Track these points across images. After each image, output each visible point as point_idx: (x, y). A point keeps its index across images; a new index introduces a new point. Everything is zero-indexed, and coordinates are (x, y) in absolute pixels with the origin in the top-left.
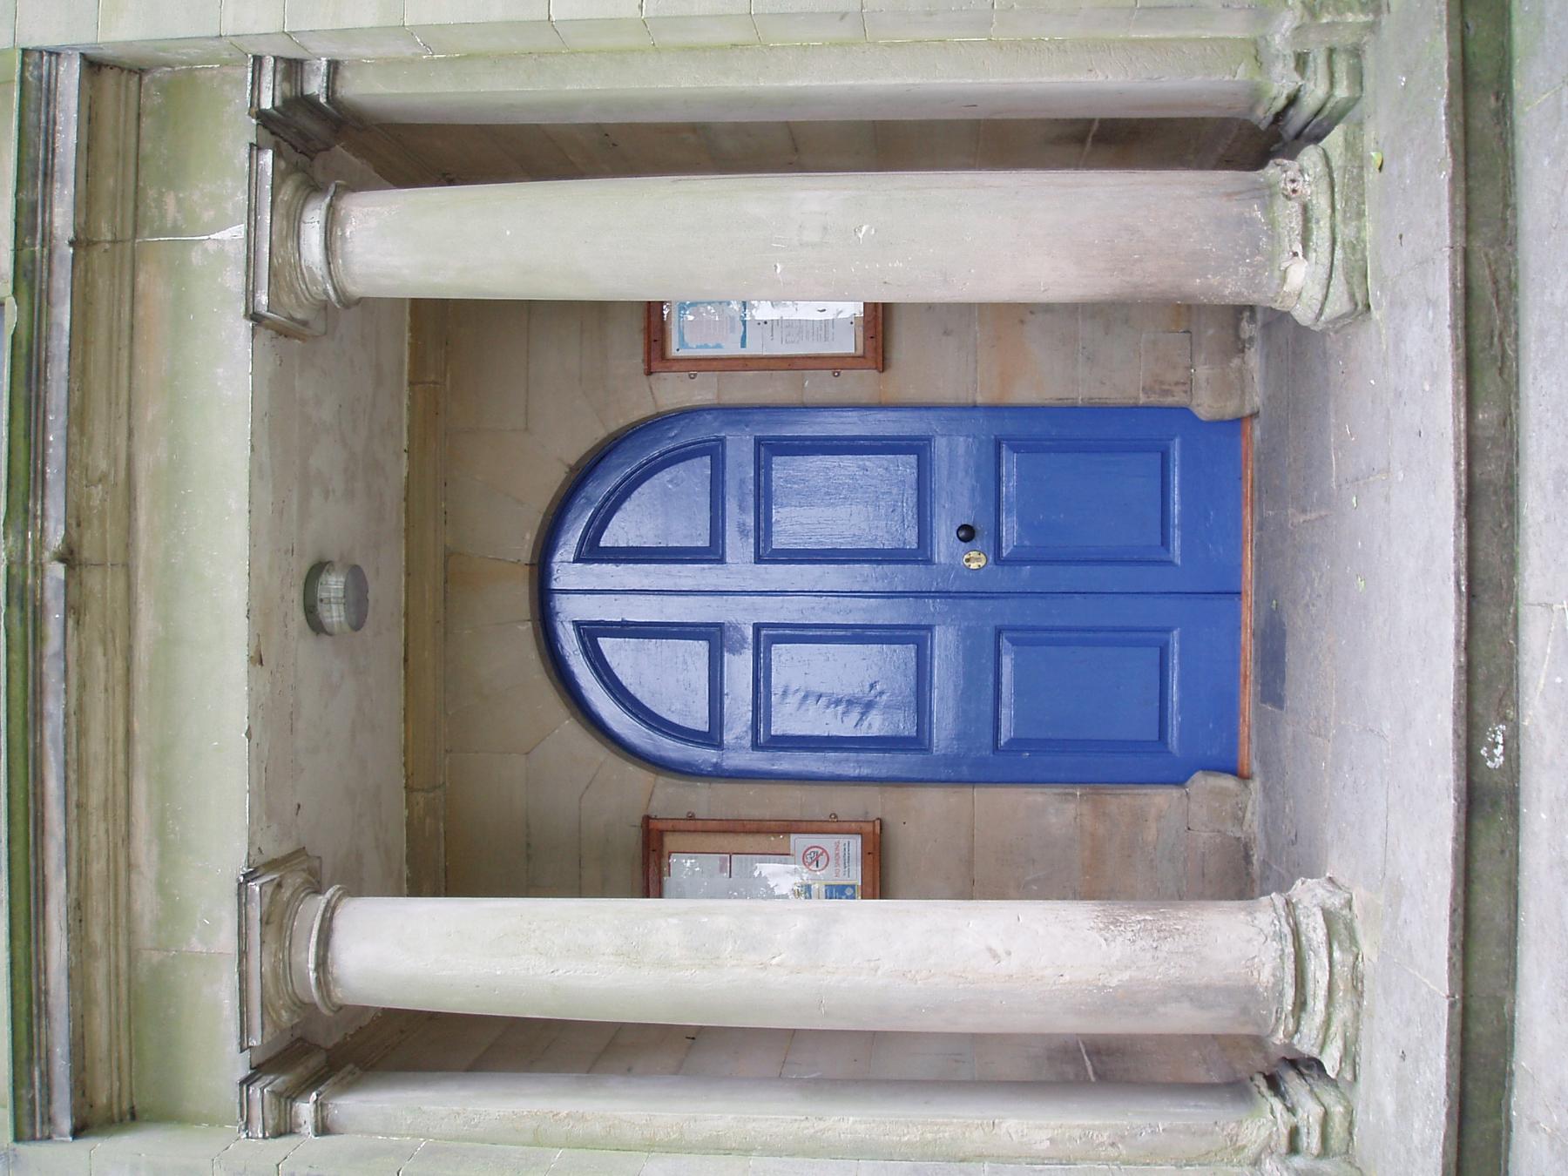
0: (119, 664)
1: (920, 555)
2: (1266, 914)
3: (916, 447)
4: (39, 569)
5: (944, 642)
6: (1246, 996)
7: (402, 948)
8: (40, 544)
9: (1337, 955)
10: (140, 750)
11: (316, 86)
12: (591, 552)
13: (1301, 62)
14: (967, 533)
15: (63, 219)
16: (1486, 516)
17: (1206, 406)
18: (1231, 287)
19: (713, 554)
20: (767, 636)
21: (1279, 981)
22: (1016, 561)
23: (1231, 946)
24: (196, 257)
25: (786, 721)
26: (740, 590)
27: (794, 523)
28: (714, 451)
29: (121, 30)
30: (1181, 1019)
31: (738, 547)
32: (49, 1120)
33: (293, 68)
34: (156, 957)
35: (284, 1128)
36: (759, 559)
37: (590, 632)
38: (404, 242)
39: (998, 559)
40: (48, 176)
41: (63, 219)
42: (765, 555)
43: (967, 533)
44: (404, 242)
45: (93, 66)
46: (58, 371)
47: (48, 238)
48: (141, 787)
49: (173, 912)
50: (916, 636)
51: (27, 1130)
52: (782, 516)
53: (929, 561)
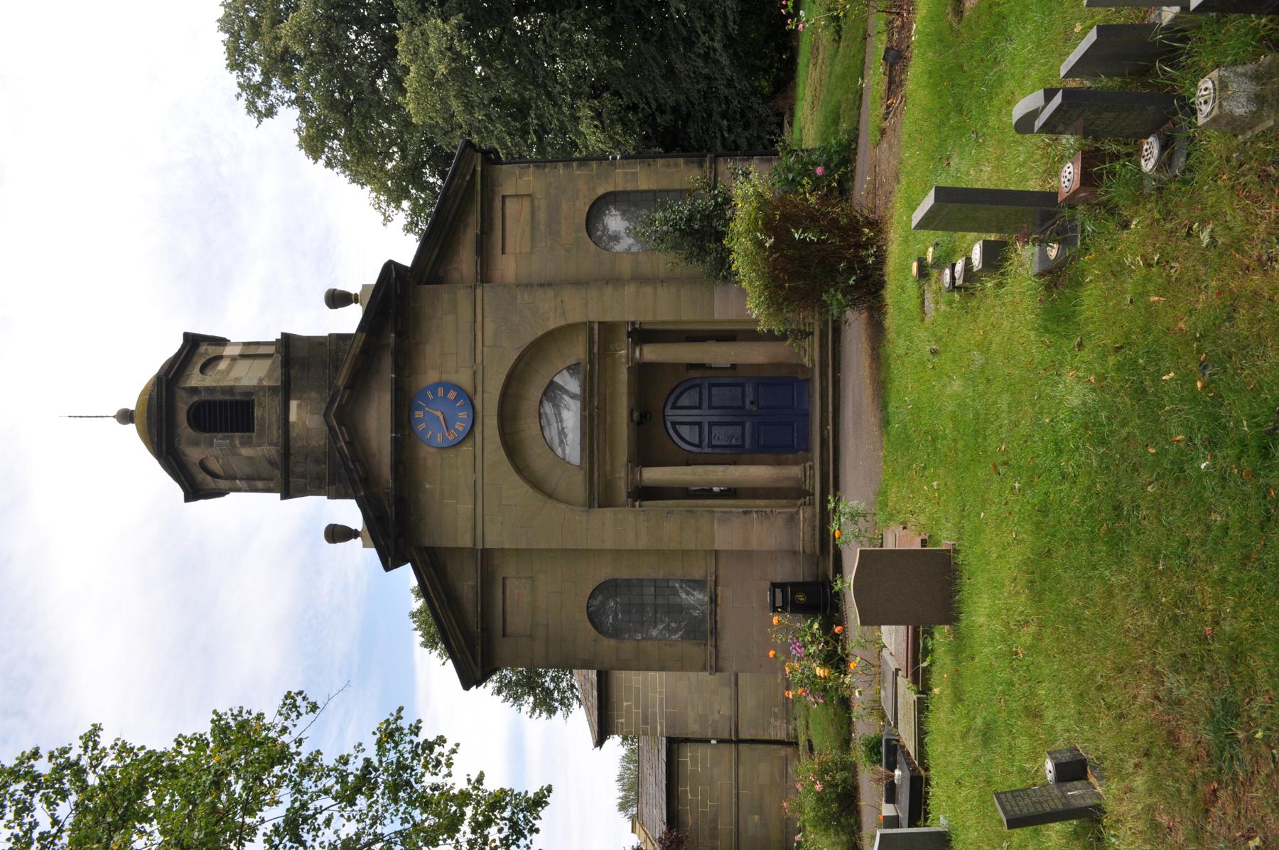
1: (743, 407)
2: (801, 467)
5: (748, 425)
7: (654, 475)
12: (674, 407)
15: (596, 350)
18: (794, 361)
19: (700, 407)
20: (711, 424)
23: (795, 471)
25: (715, 442)
26: (705, 416)
27: (715, 402)
28: (700, 386)
29: (607, 319)
30: (787, 484)
31: (705, 404)
33: (633, 323)
37: (674, 424)
38: (651, 353)
41: (596, 350)
42: (710, 407)
44: (651, 353)
50: (742, 424)
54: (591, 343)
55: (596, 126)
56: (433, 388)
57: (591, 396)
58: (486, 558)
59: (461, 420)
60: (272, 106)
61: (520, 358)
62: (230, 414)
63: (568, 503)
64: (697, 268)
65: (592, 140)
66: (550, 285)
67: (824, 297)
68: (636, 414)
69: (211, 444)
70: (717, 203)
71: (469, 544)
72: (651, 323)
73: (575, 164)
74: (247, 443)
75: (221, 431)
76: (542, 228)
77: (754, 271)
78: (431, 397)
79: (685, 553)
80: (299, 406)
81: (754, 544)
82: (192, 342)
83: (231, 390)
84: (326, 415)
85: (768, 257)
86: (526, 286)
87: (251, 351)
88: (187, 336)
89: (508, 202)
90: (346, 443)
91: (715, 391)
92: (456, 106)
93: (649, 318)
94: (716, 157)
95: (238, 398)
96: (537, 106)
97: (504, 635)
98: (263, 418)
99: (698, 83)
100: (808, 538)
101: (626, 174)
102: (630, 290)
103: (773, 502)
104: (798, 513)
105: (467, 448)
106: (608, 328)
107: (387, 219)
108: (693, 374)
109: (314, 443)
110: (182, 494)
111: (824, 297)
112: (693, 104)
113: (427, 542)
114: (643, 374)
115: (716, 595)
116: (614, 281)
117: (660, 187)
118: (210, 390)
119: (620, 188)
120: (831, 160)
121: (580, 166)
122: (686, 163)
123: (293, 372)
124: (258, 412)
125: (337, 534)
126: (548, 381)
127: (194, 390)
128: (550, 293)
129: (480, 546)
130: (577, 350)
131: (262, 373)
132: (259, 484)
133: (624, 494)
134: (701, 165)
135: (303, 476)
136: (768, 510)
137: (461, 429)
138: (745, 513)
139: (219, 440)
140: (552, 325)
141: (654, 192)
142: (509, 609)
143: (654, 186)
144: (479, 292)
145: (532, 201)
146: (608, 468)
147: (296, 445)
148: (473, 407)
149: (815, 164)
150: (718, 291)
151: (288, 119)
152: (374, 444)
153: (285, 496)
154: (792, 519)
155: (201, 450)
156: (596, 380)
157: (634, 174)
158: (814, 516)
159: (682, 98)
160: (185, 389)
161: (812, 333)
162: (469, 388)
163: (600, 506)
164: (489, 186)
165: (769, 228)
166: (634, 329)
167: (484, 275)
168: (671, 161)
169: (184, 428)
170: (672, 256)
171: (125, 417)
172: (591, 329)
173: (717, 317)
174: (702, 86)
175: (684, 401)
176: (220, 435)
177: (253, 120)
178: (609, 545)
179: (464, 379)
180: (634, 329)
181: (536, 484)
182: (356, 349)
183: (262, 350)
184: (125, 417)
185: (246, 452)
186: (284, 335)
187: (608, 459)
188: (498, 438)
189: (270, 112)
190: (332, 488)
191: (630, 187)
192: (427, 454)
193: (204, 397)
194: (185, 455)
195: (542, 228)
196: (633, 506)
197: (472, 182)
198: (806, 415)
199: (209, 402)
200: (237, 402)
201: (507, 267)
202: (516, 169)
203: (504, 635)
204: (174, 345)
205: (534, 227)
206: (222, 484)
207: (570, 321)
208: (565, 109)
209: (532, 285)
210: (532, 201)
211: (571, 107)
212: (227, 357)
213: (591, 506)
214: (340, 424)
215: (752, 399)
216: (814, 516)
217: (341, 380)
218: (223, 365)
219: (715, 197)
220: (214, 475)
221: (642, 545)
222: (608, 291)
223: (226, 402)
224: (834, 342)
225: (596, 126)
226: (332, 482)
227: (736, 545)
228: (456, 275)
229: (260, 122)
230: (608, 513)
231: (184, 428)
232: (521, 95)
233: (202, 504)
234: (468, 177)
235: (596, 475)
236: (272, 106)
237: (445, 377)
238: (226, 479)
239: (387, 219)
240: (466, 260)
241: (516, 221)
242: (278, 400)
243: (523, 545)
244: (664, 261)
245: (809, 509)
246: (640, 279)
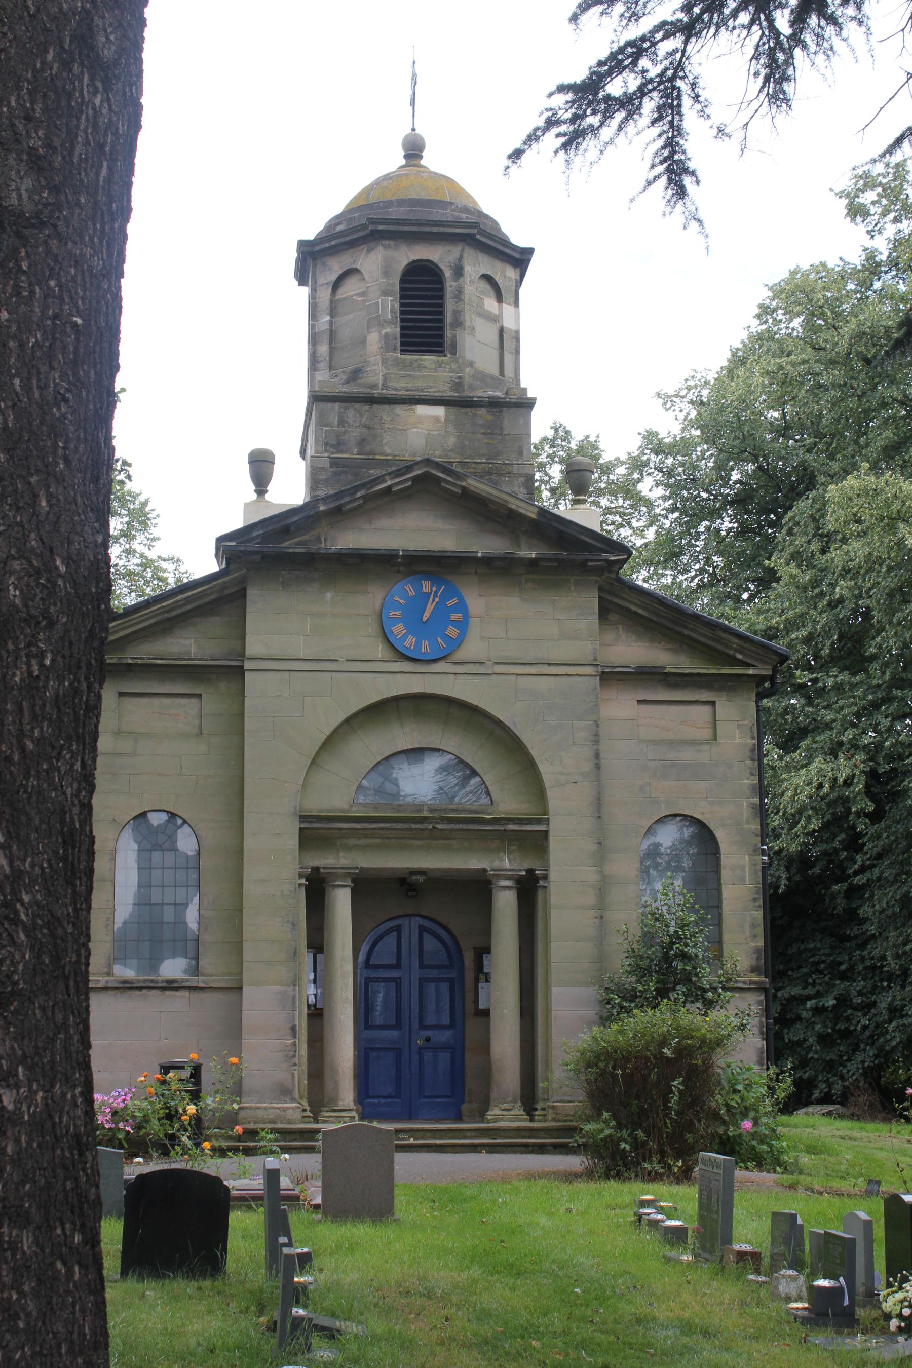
1: (422, 1027)
2: (352, 1105)
3: (452, 1025)
4: (430, 823)
5: (395, 1033)
6: (335, 1099)
7: (341, 902)
8: (437, 823)
10: (387, 841)
11: (541, 883)
12: (422, 930)
13: (543, 1109)
14: (428, 1039)
15: (511, 827)
17: (465, 1107)
18: (494, 1095)
19: (422, 966)
20: (398, 982)
22: (420, 1054)
23: (347, 1095)
24: (501, 854)
27: (431, 988)
29: (554, 843)
32: (303, 822)
33: (545, 877)
34: (338, 844)
35: (301, 876)
36: (420, 979)
37: (398, 929)
38: (505, 902)
39: (420, 1048)
41: (511, 827)
43: (428, 1039)
44: (505, 902)
45: (547, 832)
46: (476, 827)
48: (378, 841)
49: (348, 848)
52: (433, 985)
53: (420, 1029)
54: (520, 821)
55: (820, 786)
56: (462, 607)
57: (450, 820)
58: (231, 672)
59: (418, 644)
60: (866, 214)
61: (499, 723)
62: (424, 317)
63: (304, 786)
64: (619, 964)
65: (799, 778)
66: (598, 766)
67: (606, 1115)
68: (421, 878)
69: (385, 293)
70: (705, 991)
71: (249, 652)
72: (546, 901)
73: (756, 800)
74: (387, 346)
75: (402, 305)
76: (672, 755)
77: (635, 1036)
78: (450, 603)
79: (238, 946)
80: (437, 419)
81: (248, 1040)
82: (520, 259)
83: (458, 324)
84: (428, 462)
85: (649, 1050)
86: (597, 735)
87: (507, 342)
88: (529, 252)
89: (707, 709)
90: (389, 488)
91: (445, 987)
92: (858, 549)
93: (554, 899)
94: (765, 990)
95: (448, 333)
96: (853, 686)
97: (121, 694)
98: (421, 368)
99: (897, 956)
100: (260, 1114)
101: (743, 868)
102: (590, 874)
103: (305, 1067)
104: (293, 1100)
105: (380, 650)
106: (538, 843)
107: (668, 400)
108: (469, 958)
109: (387, 438)
110: (311, 237)
111: (606, 1115)
112: (862, 946)
113: (253, 593)
114: (479, 888)
115: (177, 989)
116: (602, 852)
117: (724, 915)
118: (459, 295)
119: (724, 860)
120: (762, 1142)
121: (753, 806)
122: (757, 951)
123: (482, 412)
124: (429, 359)
125: (261, 467)
126: (477, 767)
127: (459, 272)
128: (587, 767)
129: (247, 665)
130: (508, 802)
131: (480, 365)
132: (323, 349)
133: (316, 863)
134: (754, 970)
135: (342, 422)
136: (296, 1060)
137: (407, 644)
138: (293, 1029)
139: (390, 305)
140: (544, 768)
141: (719, 907)
142: (156, 701)
143: (725, 904)
144: (589, 670)
145: (707, 742)
146: (351, 841)
147: (383, 412)
148: (435, 661)
149: (756, 1122)
150: (593, 993)
151: (844, 244)
152: (384, 522)
153: (317, 398)
154: (285, 1092)
155: (378, 271)
156: (470, 827)
157: (743, 880)
158: (289, 1122)
159: (873, 929)
160: (461, 258)
161: (532, 1120)
162: (459, 656)
163: (300, 829)
164: (729, 684)
165: (682, 1052)
166: (537, 879)
167: (610, 677)
168: (760, 930)
169: (407, 255)
170: (636, 931)
171: (414, 150)
172: (539, 821)
173: (555, 990)
174: (892, 965)
175: (430, 943)
176: (397, 305)
177: (846, 183)
178: (249, 843)
179: (472, 648)
180: (537, 879)
181: (331, 742)
182: (514, 504)
183: (508, 358)
184: (414, 150)
185: (374, 340)
186: (535, 399)
187: (363, 841)
188: (394, 693)
189: (856, 211)
190: (326, 463)
191: (725, 874)
192: (371, 597)
193: (450, 285)
194: (369, 251)
195: (672, 755)
196: (301, 876)
197: (733, 662)
198: (411, 1118)
199: (442, 289)
200: (442, 329)
201: (621, 707)
202: (751, 719)
203: (121, 694)
204: (518, 239)
205: (673, 744)
206: (325, 295)
207: (551, 794)
208: (850, 734)
209: (597, 742)
210: (707, 742)
211: (855, 746)
212: (501, 310)
213: (303, 818)
214: (415, 479)
215: (433, 1039)
216: (289, 1122)
217: (474, 484)
218: (490, 304)
219: (715, 990)
220: (337, 285)
221: (250, 888)
222: (590, 846)
223: (441, 313)
224: (526, 1145)
225: (820, 786)
226: (334, 463)
227: (248, 1016)
228: (610, 636)
229: (840, 194)
230: (295, 841)
231: (407, 255)
232: (874, 657)
233: (292, 255)
234: (739, 656)
236: (866, 214)
237: (474, 623)
238: (332, 301)
239: (668, 400)
240: (632, 651)
241: (684, 719)
242: (449, 394)
243: (250, 724)
244: (627, 920)
245: (298, 1115)
246: (602, 889)
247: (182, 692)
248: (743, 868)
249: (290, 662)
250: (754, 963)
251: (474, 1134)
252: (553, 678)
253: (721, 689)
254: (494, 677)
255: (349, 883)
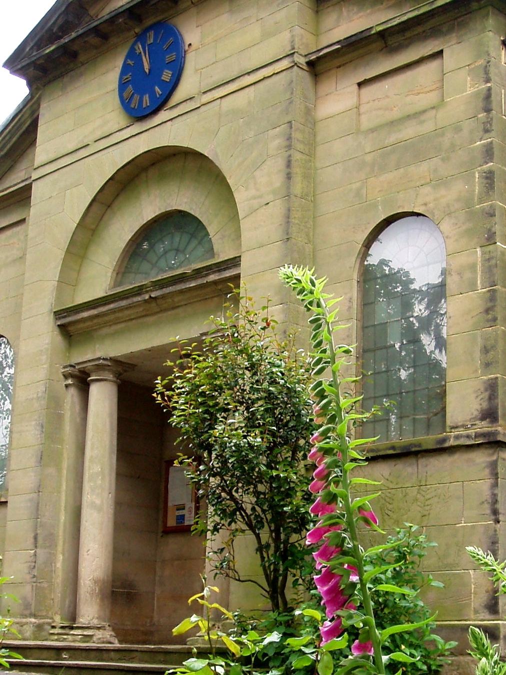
0: (143, 314)
4: (147, 292)
8: (151, 291)
9: (80, 637)
16: (98, 654)
21: (79, 623)
32: (60, 318)
40: (219, 271)
47: (207, 275)
48: (122, 325)
51: (57, 314)
101: (473, 267)
157: (473, 287)
167: (317, 67)
195: (393, 139)
201: (340, 98)
205: (392, 124)
235: (85, 314)
247: (15, 220)
248: (473, 267)
249: (59, 161)
250: (485, 405)
251: (118, 655)
252: (253, 87)
253: (435, 33)
254: (203, 108)
255: (110, 377)
